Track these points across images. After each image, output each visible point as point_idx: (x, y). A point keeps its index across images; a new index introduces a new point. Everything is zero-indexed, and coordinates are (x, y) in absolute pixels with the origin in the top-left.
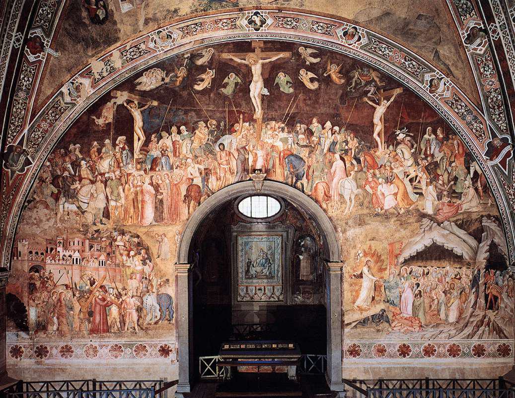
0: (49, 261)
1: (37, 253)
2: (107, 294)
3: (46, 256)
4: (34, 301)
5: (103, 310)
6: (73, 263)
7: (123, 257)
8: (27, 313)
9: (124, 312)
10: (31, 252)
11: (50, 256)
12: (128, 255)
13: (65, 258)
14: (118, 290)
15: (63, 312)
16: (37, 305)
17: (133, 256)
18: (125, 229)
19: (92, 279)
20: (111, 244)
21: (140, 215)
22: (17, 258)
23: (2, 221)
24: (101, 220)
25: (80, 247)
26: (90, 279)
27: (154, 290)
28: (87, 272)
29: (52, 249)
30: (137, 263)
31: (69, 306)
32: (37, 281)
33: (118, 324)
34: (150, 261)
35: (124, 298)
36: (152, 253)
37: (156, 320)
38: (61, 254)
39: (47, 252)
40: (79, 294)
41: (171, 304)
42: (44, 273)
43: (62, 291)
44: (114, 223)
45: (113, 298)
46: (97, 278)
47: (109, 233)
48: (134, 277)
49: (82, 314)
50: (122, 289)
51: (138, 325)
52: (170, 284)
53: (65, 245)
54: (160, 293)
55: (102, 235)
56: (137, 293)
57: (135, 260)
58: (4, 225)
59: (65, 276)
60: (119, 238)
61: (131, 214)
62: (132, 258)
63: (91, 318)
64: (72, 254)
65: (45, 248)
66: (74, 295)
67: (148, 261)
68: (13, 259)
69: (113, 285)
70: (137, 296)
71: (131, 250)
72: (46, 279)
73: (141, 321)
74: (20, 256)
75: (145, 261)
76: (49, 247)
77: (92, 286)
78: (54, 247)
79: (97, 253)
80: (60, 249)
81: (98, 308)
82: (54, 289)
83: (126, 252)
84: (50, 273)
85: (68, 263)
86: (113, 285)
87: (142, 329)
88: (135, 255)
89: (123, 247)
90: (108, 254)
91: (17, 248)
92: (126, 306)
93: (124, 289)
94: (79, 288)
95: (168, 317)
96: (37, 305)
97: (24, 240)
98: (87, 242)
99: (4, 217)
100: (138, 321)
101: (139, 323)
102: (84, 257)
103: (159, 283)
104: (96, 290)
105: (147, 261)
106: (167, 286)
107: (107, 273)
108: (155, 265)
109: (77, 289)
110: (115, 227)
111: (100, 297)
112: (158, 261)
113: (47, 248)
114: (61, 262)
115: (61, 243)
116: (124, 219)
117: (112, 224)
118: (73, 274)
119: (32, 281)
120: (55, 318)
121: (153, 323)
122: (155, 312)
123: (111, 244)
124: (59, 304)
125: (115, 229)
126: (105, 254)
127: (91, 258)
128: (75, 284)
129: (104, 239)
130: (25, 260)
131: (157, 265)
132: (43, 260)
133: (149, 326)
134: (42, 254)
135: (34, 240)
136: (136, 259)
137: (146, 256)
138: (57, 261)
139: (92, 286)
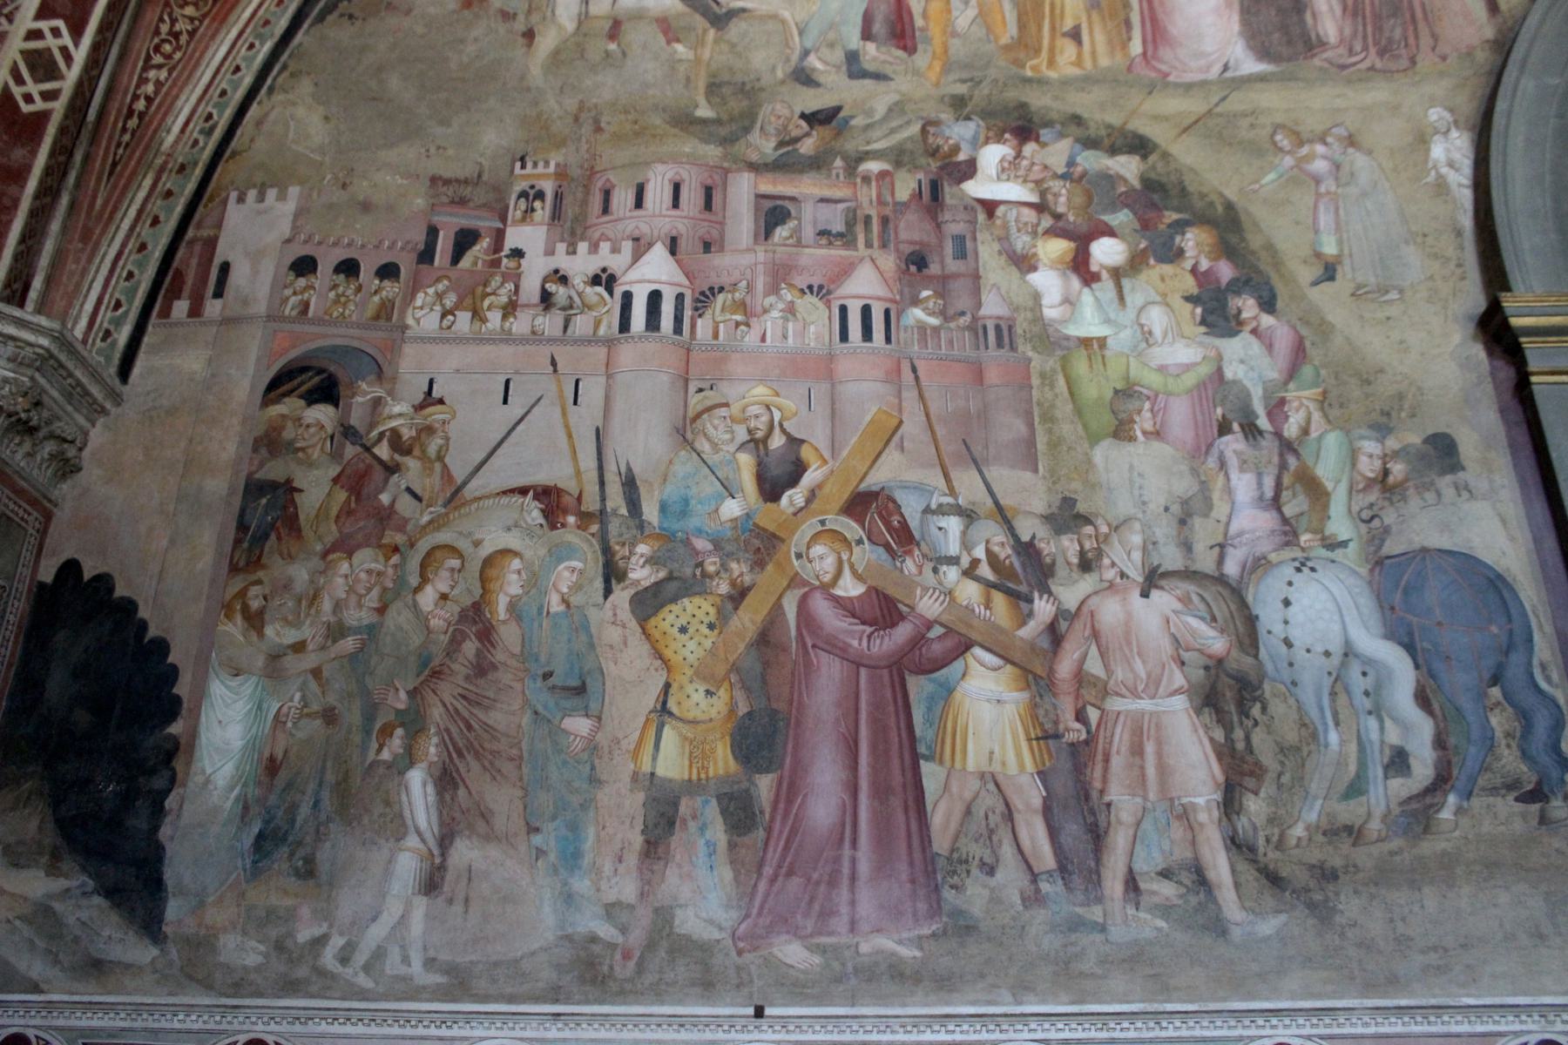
0: (423, 317)
1: (349, 268)
2: (910, 566)
3: (415, 288)
4: (255, 621)
5: (877, 706)
6: (625, 325)
7: (1034, 278)
8: (176, 728)
9: (1080, 716)
10: (304, 266)
11: (440, 287)
12: (1080, 266)
13: (560, 292)
14: (1011, 530)
15: (497, 718)
16: (275, 657)
17: (1117, 274)
18: (1038, 100)
19: (777, 441)
20: (933, 198)
21: (1135, 19)
22: (195, 311)
23: (158, 59)
24: (852, 57)
25: (683, 222)
26: (757, 443)
27: (1340, 525)
28: (729, 391)
29: (465, 240)
30: (1157, 319)
31: (559, 668)
32: (311, 465)
33: (1035, 834)
34: (1268, 304)
35: (1071, 590)
36: (1270, 247)
37: (1401, 787)
38: (534, 270)
39: (426, 256)
40: (651, 561)
41: (1518, 640)
42: (377, 403)
43: (512, 541)
44: (947, 68)
45: (970, 592)
46: (816, 434)
47: (915, 129)
48: (1144, 421)
49: (668, 733)
50: (1048, 519)
51: (1235, 844)
52: (1471, 474)
53: (570, 210)
54: (1392, 547)
55: (852, 145)
56: (1187, 547)
57: (1135, 298)
58: (159, 84)
59: (545, 415)
60: (993, 155)
61: (1068, 24)
62: (1107, 285)
63: (765, 785)
64: (616, 263)
65: (420, 237)
66: (612, 574)
67: (1248, 306)
68: (166, 313)
69: (969, 487)
70: (1189, 575)
71: (1110, 232)
72: (383, 451)
73: (1255, 807)
74: (218, 294)
75: (1223, 306)
76: (450, 224)
77: (771, 490)
78: (486, 223)
79: (816, 258)
80: (528, 236)
81: (829, 674)
82: (436, 524)
83: (1058, 248)
84: (430, 399)
85: (581, 325)
86: (969, 487)
87: (1274, 879)
88: (1136, 263)
89: (1029, 215)
90: (917, 261)
91: (211, 244)
92: (1094, 667)
93: (1067, 517)
94: (663, 508)
95: (1509, 760)
96: (275, 657)
97: (271, 194)
98: (743, 190)
99: (176, 35)
100: (1230, 804)
101: (1242, 823)
102: (716, 281)
103: (1368, 467)
104: (809, 527)
105: (1235, 302)
106: (1449, 493)
107: (910, 395)
108: (1304, 332)
109: (641, 526)
110: (961, 89)
111: (850, 588)
112: (1330, 301)
113: (433, 232)
114: (520, 324)
115: (540, 195)
116: (1025, 44)
117: (933, 76)
118: (619, 405)
119: (275, 470)
120: (416, 778)
121: (1375, 825)
122: (1377, 712)
123: (933, 198)
124: (470, 647)
125: (959, 105)
126: (889, 262)
127: (774, 289)
128: (630, 484)
129: (873, 166)
130: (250, 319)
131: (1324, 330)
132: (385, 311)
133: (1345, 846)
134: (388, 271)
135: (344, 186)
136: (1139, 290)
137: (1226, 271)
138: (494, 318)
139: (771, 490)
